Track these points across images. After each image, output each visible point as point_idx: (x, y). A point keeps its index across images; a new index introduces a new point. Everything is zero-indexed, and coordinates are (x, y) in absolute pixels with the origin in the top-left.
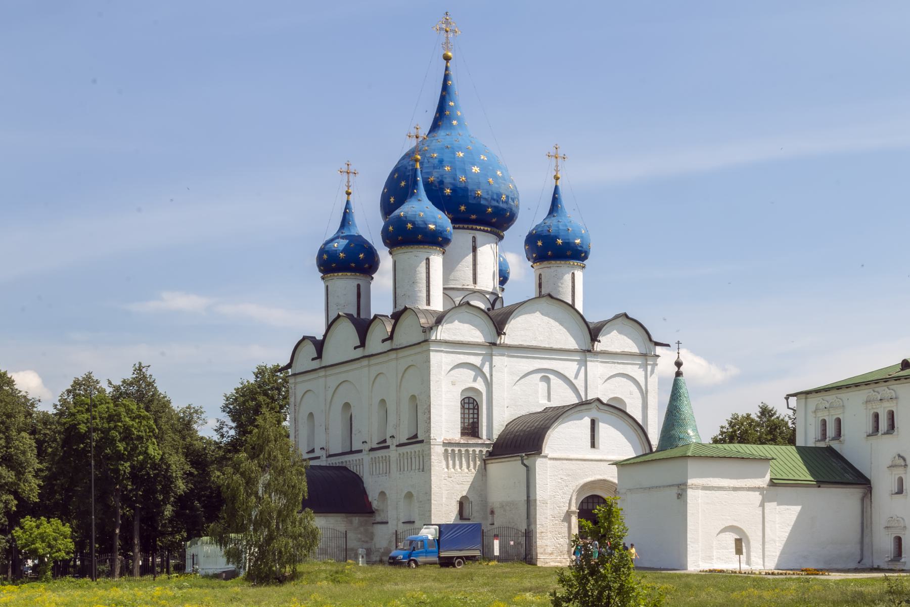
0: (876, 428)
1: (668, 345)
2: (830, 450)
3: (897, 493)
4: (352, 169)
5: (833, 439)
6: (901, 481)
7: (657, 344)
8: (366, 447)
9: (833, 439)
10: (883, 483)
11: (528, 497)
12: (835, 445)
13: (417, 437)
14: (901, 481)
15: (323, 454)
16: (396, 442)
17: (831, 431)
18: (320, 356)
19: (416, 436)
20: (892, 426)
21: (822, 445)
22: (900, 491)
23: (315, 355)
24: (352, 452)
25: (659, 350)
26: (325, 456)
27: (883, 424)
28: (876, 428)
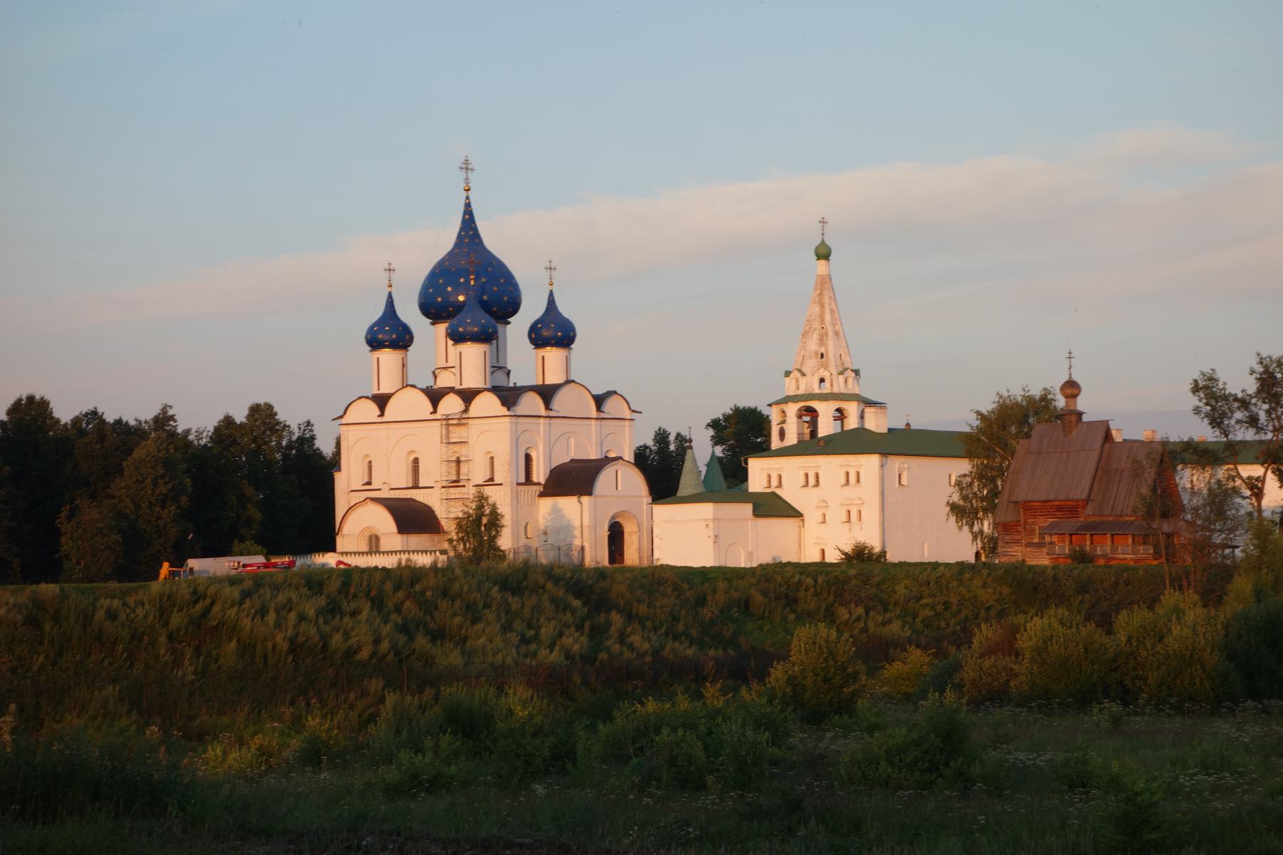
0: (807, 484)
1: (641, 413)
2: (773, 493)
3: (822, 523)
4: (392, 267)
5: (776, 487)
6: (824, 515)
7: (634, 411)
8: (439, 485)
9: (776, 487)
10: (812, 516)
11: (582, 524)
12: (778, 491)
13: (493, 481)
14: (824, 515)
15: (386, 488)
16: (472, 483)
17: (774, 482)
18: (382, 415)
19: (492, 479)
20: (817, 484)
21: (769, 490)
22: (824, 522)
23: (379, 413)
24: (416, 486)
25: (635, 416)
26: (387, 490)
27: (812, 481)
28: (807, 484)
